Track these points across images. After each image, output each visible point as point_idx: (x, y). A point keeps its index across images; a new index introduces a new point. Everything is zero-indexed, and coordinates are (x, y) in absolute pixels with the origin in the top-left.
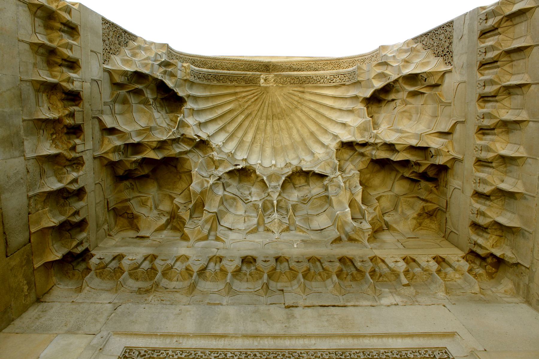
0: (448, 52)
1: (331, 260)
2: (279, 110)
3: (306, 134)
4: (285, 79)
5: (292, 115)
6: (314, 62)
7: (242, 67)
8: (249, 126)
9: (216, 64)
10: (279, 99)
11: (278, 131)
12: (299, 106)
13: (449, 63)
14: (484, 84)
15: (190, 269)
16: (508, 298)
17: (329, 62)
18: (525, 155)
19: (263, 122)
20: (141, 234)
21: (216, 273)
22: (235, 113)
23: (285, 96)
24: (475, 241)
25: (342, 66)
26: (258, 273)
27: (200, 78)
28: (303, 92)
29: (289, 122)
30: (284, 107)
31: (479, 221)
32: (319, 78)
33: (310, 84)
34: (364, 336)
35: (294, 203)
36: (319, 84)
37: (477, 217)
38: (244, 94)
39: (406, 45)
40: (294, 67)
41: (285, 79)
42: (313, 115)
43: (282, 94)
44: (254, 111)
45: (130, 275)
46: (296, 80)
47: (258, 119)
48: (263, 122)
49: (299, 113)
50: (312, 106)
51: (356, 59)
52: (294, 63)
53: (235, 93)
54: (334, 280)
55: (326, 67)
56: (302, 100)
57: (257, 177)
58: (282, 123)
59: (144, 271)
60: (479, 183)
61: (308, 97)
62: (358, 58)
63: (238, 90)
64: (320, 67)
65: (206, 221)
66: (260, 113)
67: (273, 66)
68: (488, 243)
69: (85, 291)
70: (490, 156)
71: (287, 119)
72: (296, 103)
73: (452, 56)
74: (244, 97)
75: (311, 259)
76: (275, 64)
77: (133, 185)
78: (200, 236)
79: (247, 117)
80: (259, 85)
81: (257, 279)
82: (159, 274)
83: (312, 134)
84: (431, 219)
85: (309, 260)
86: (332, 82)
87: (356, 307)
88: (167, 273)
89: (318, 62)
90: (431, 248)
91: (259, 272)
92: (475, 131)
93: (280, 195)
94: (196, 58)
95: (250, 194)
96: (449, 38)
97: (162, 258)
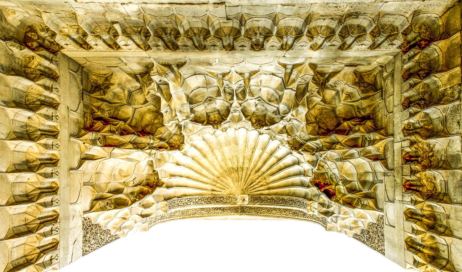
0: (87, 229)
1: (185, 47)
2: (233, 175)
3: (210, 155)
4: (228, 201)
5: (222, 171)
6: (204, 215)
7: (263, 210)
8: (257, 162)
9: (285, 213)
10: (232, 185)
12: (216, 179)
13: (86, 220)
14: (52, 203)
15: (309, 38)
16: (11, 6)
17: (191, 216)
18: (8, 142)
19: (246, 166)
20: (352, 69)
21: (286, 34)
22: (269, 172)
23: (227, 187)
24: (52, 63)
25: (181, 213)
26: (250, 35)
27: (298, 202)
28: (213, 190)
29: (224, 166)
30: (228, 178)
31: (50, 81)
32: (199, 202)
33: (207, 197)
35: (219, 98)
36: (200, 197)
37: (52, 85)
38: (262, 188)
39: (125, 233)
40: (220, 211)
41: (228, 201)
42: (204, 172)
44: (253, 175)
45: (365, 30)
46: (219, 200)
47: (250, 168)
48: (246, 166)
49: (216, 173)
50: (205, 179)
51: (169, 219)
52: (220, 214)
53: (269, 189)
54: (182, 29)
55: (194, 212)
56: (213, 183)
57: (250, 120)
58: (230, 165)
59: (351, 35)
60: (52, 116)
61: (209, 187)
62: (167, 220)
63: (267, 192)
64: (199, 212)
65: (294, 81)
66: (249, 173)
67: (237, 212)
68: (38, 61)
69: (410, 12)
70: (44, 141)
71: (226, 168)
72: (219, 181)
73: (84, 225)
74: (262, 186)
75: (204, 49)
76: (237, 213)
77: (358, 112)
78: (300, 68)
79: (259, 169)
80: (250, 196)
81: (250, 29)
82: (337, 32)
83: (205, 156)
84: (97, 83)
85: (205, 47)
86: (189, 199)
87: (161, 2)
88: (331, 33)
89: (200, 215)
90: (94, 57)
91: (249, 36)
92: (59, 162)
93: (231, 104)
94: (302, 218)
95: (256, 105)
96: (86, 241)
97: (334, 47)
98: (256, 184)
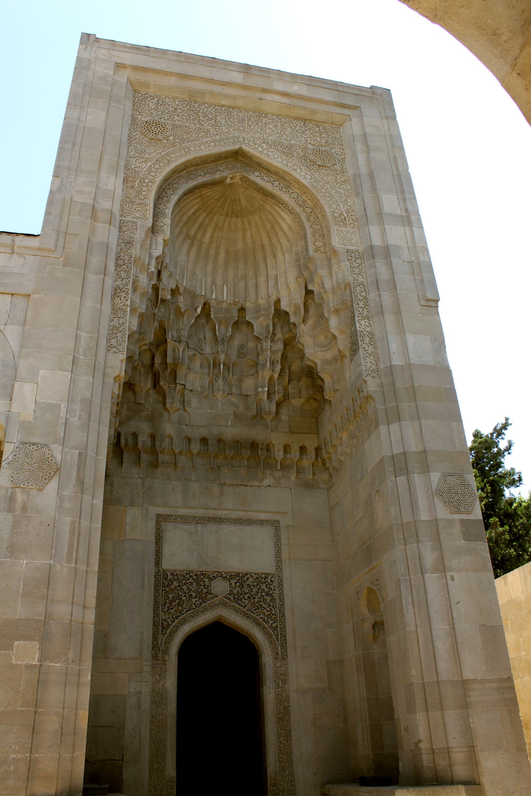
2: (239, 209)
4: (251, 183)
10: (241, 197)
11: (234, 230)
17: (296, 181)
22: (198, 213)
29: (246, 223)
30: (244, 207)
34: (250, 511)
36: (280, 205)
43: (245, 193)
48: (222, 217)
67: (243, 152)
74: (208, 196)
79: (207, 215)
83: (263, 246)
98: (214, 196)
